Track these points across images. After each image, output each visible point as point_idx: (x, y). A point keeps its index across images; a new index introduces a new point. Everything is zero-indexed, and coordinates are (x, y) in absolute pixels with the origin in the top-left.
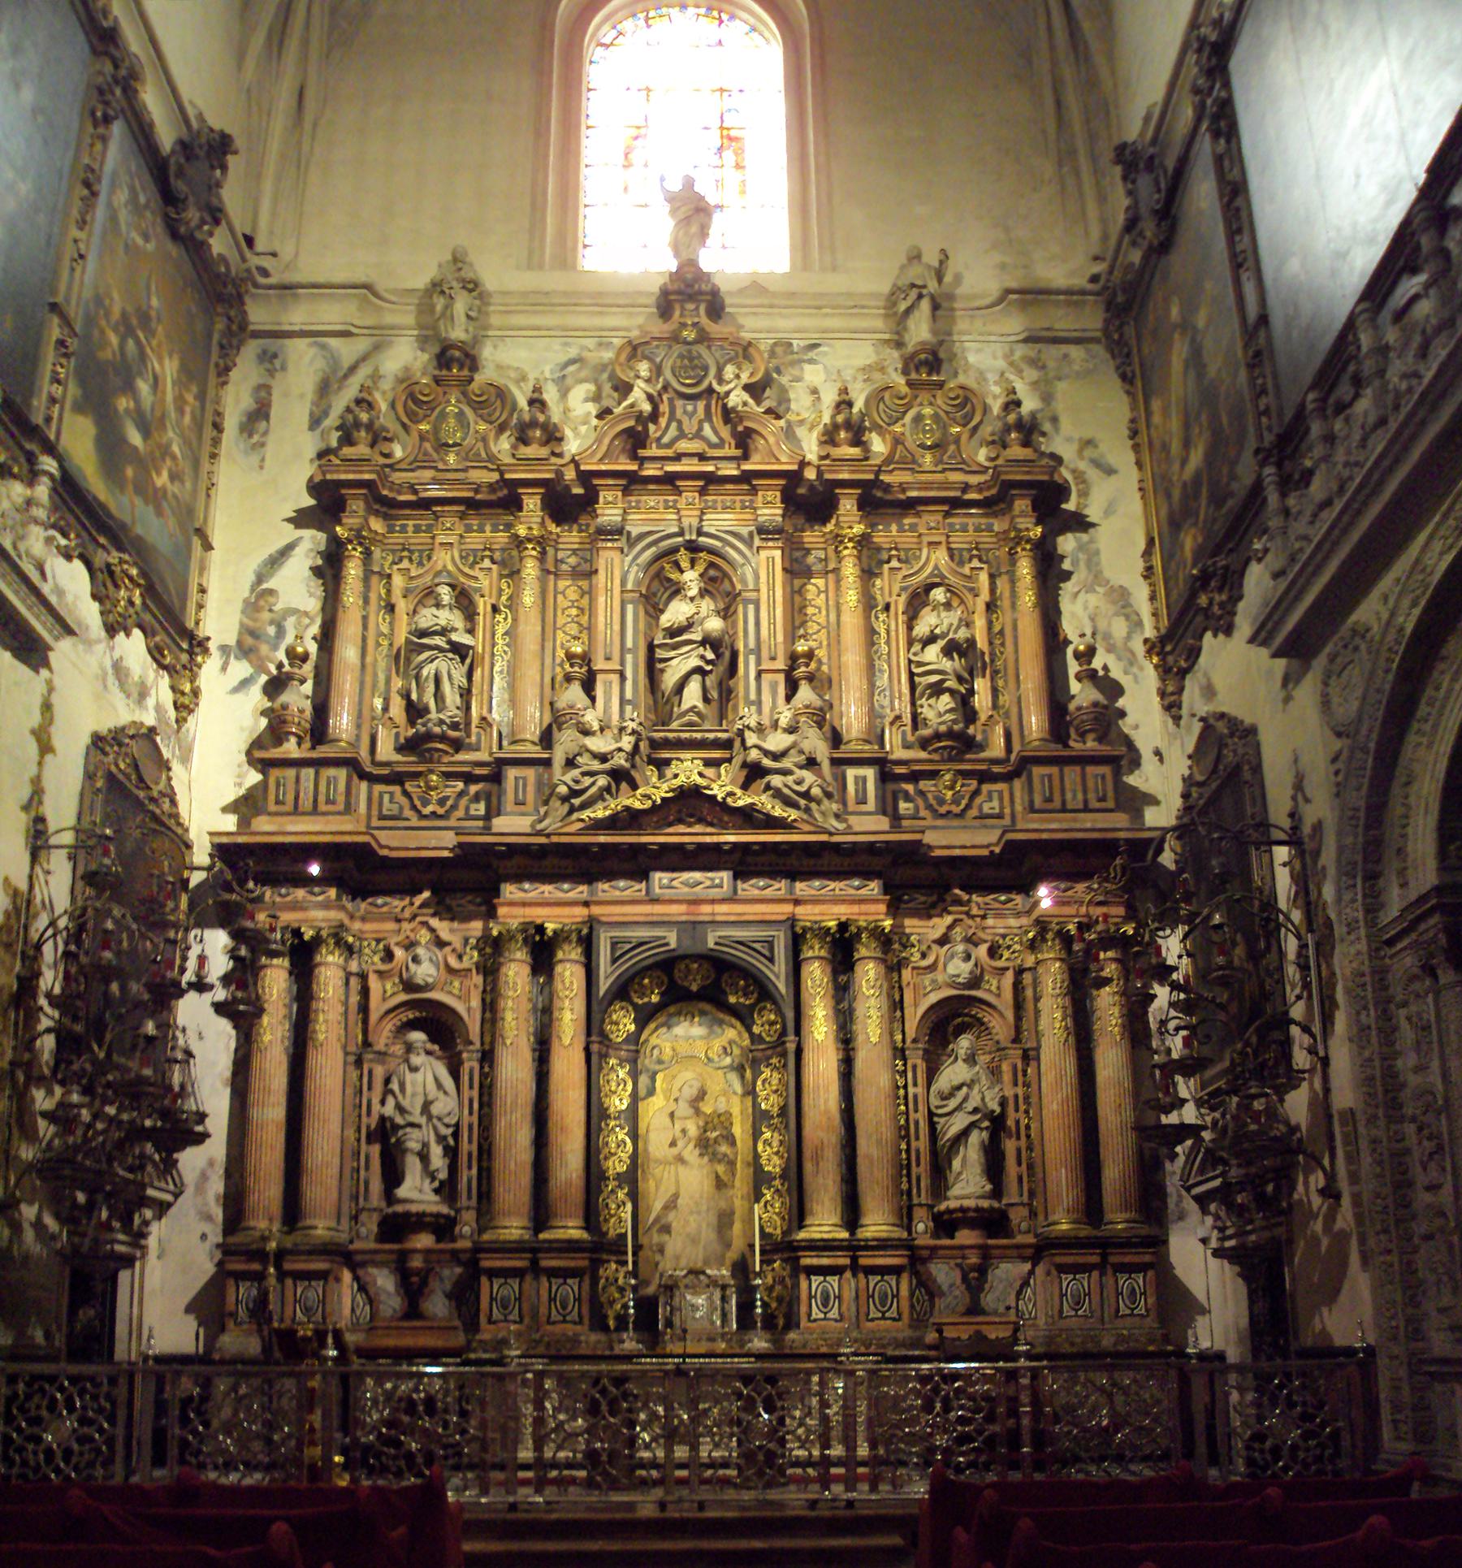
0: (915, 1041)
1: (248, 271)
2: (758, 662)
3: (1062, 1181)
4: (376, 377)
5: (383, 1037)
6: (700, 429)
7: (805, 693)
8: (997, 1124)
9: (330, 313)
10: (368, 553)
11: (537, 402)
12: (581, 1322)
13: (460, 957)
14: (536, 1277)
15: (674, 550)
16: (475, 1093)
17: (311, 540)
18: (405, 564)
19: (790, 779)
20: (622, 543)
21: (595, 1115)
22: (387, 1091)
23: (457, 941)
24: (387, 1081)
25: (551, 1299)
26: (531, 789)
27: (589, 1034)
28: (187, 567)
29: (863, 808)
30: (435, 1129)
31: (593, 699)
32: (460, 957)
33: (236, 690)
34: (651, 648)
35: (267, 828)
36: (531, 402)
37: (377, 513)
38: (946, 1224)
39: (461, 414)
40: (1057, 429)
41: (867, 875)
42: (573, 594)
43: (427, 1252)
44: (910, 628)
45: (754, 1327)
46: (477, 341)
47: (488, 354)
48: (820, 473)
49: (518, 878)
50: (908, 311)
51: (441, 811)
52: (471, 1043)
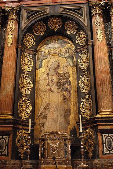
12: (8, 156)
21: (19, 72)
45: (81, 158)
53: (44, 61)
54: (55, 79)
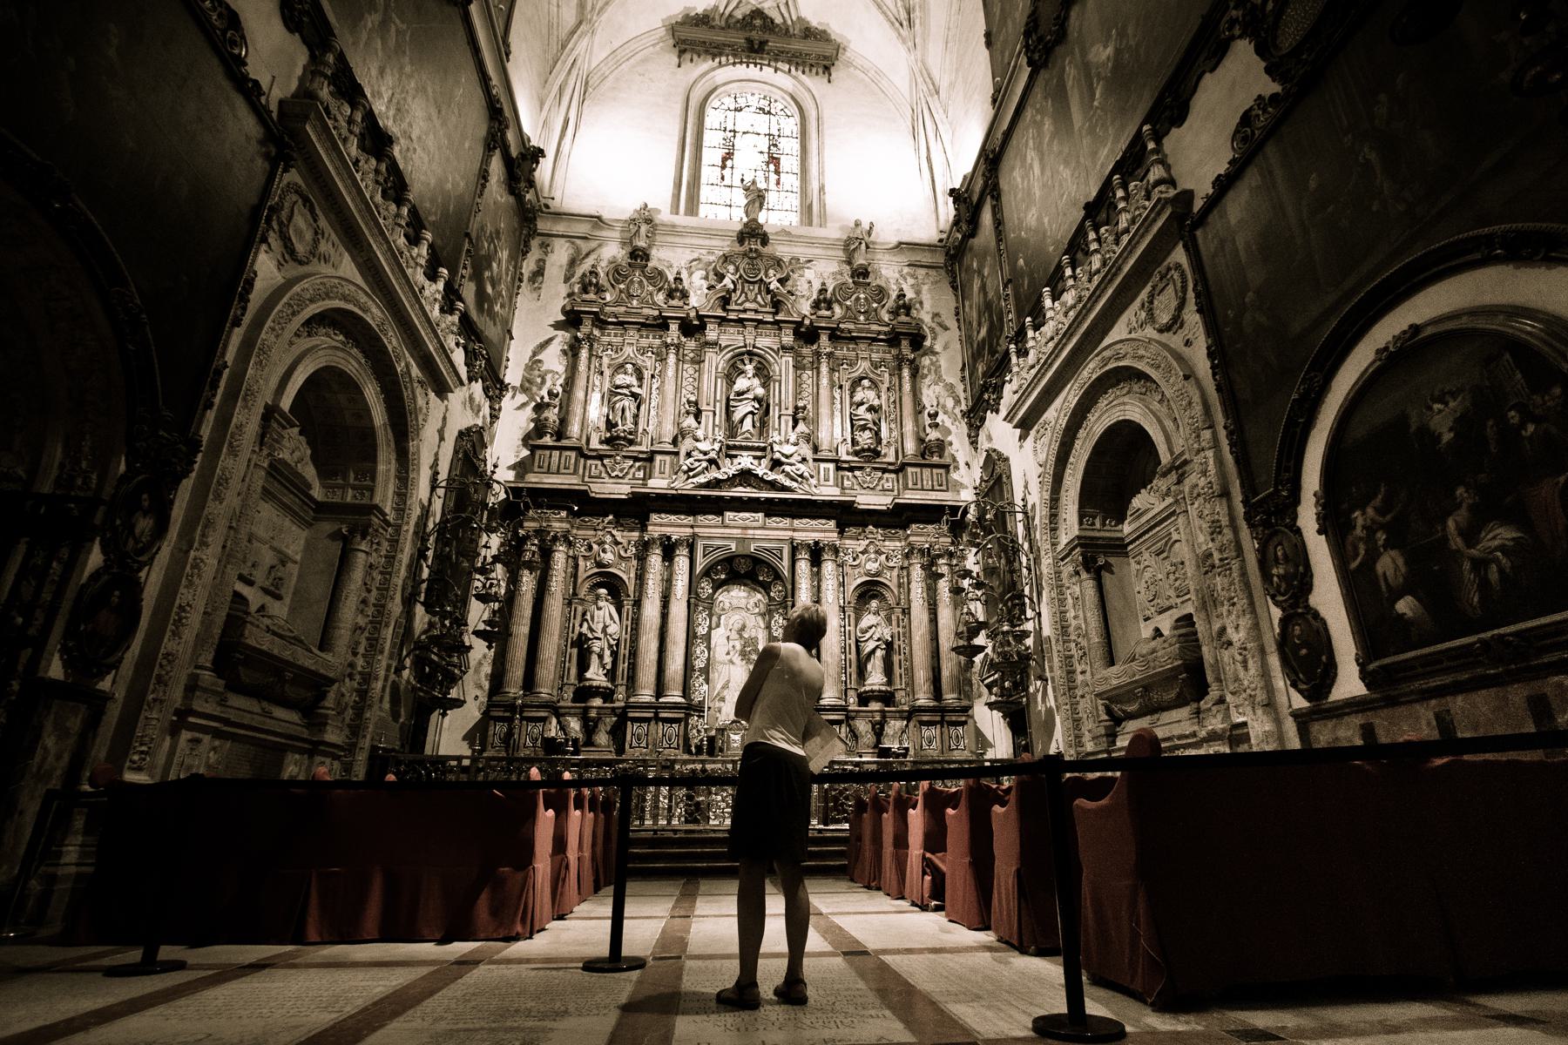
0: (849, 603)
1: (540, 206)
2: (780, 411)
3: (922, 675)
4: (598, 260)
5: (583, 592)
6: (756, 297)
7: (801, 427)
8: (889, 646)
9: (582, 228)
10: (591, 346)
11: (678, 279)
12: (678, 749)
13: (626, 551)
14: (657, 723)
15: (742, 354)
16: (629, 623)
17: (562, 337)
18: (609, 352)
19: (793, 468)
20: (717, 349)
22: (584, 620)
23: (624, 541)
24: (584, 614)
25: (664, 735)
26: (667, 466)
27: (690, 594)
28: (503, 348)
29: (827, 483)
30: (608, 640)
31: (699, 423)
32: (626, 551)
33: (519, 408)
34: (728, 400)
35: (534, 480)
36: (676, 279)
37: (597, 327)
38: (864, 699)
39: (641, 281)
40: (922, 308)
41: (829, 518)
42: (691, 371)
43: (599, 708)
44: (852, 397)
46: (650, 246)
47: (654, 252)
48: (811, 322)
49: (659, 512)
50: (854, 250)
51: (621, 475)
52: (629, 596)
53: (723, 617)
54: (738, 647)
